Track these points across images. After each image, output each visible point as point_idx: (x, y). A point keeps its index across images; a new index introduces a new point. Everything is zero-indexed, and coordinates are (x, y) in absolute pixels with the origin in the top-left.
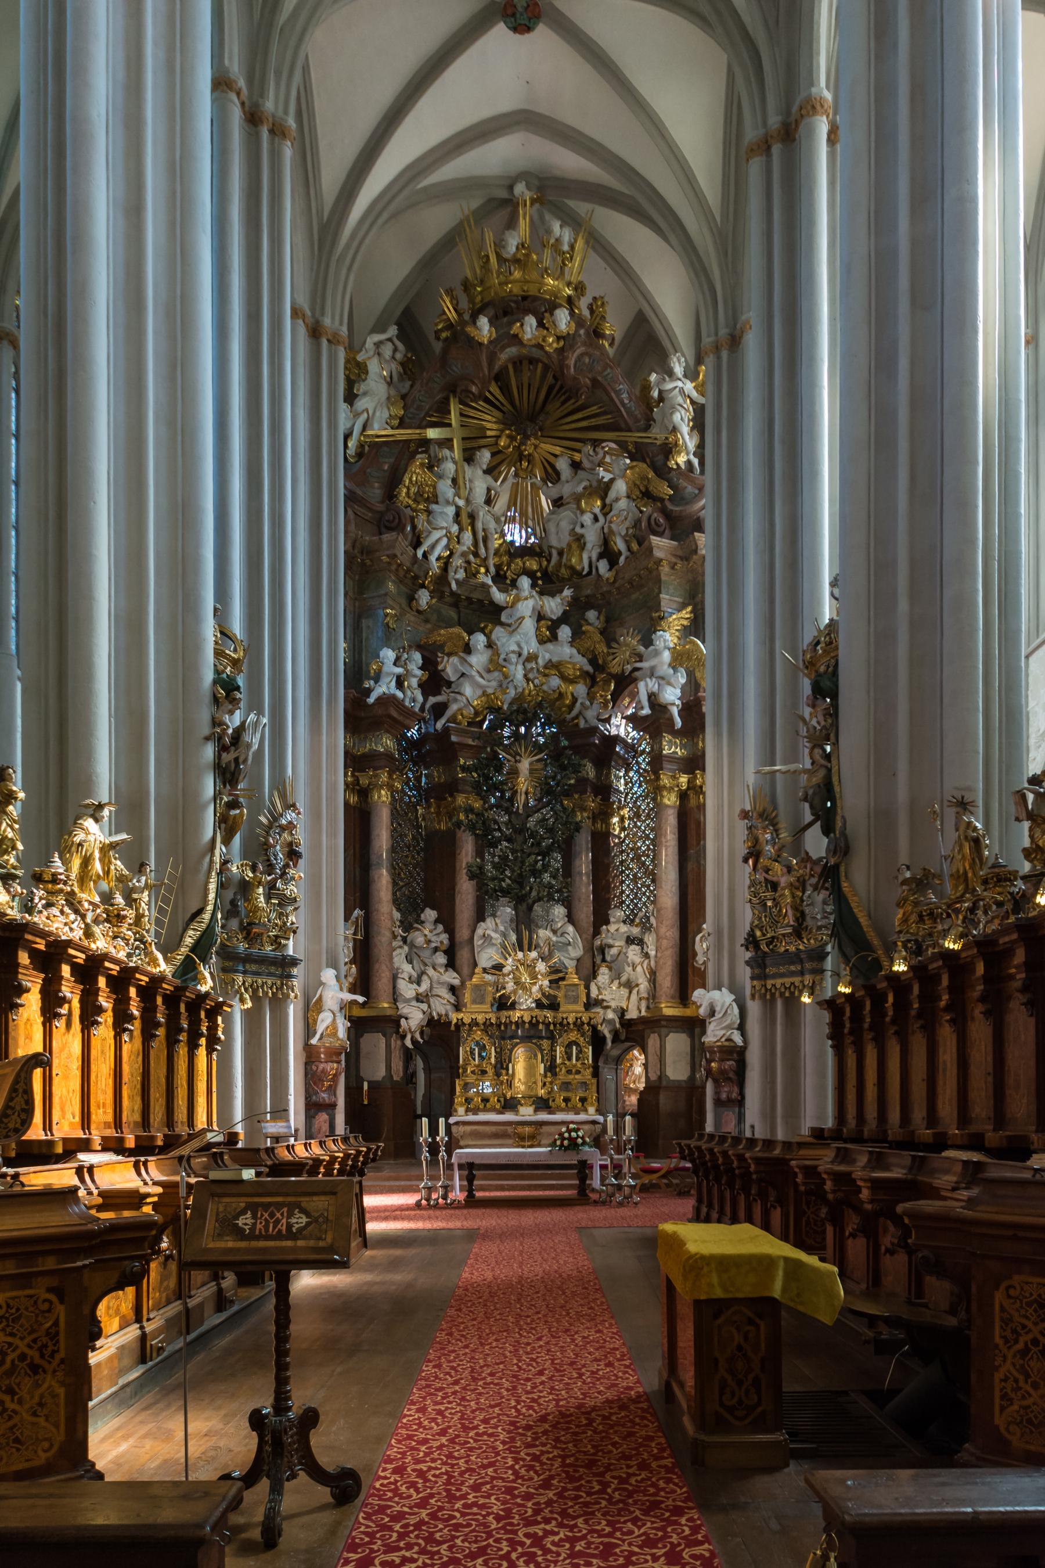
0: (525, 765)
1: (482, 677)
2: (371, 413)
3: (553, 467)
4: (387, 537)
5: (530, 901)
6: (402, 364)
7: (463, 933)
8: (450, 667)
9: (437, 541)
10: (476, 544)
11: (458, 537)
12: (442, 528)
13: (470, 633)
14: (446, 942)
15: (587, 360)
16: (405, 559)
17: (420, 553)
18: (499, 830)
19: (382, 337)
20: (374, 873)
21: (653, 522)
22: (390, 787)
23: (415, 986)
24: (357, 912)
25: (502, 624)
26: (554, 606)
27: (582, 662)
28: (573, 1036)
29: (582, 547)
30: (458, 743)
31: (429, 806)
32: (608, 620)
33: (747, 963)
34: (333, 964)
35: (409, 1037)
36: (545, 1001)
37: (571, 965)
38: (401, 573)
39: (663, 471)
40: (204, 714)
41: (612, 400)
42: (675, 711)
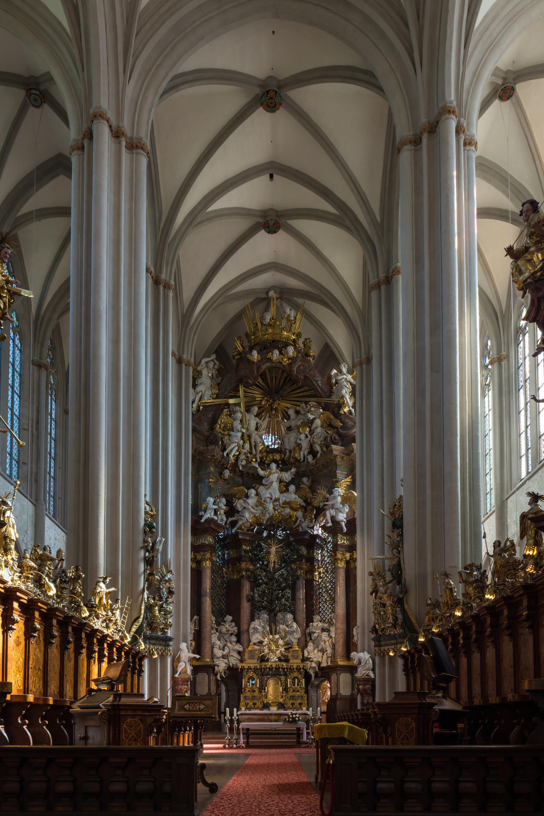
0: (273, 549)
1: (254, 509)
2: (203, 392)
3: (287, 413)
4: (210, 447)
5: (276, 612)
6: (217, 370)
7: (244, 627)
8: (239, 504)
9: (233, 448)
11: (243, 446)
12: (235, 442)
13: (248, 489)
14: (236, 631)
15: (302, 368)
16: (218, 457)
17: (225, 454)
18: (261, 579)
20: (203, 599)
21: (333, 438)
22: (211, 560)
23: (222, 651)
24: (195, 617)
25: (263, 485)
26: (287, 476)
27: (300, 501)
28: (296, 674)
29: (300, 449)
30: (242, 539)
31: (228, 568)
32: (312, 482)
33: (373, 639)
34: (185, 641)
35: (219, 675)
36: (283, 658)
37: (295, 641)
38: (217, 463)
39: (337, 415)
40: (140, 538)
41: (314, 385)
42: (343, 524)
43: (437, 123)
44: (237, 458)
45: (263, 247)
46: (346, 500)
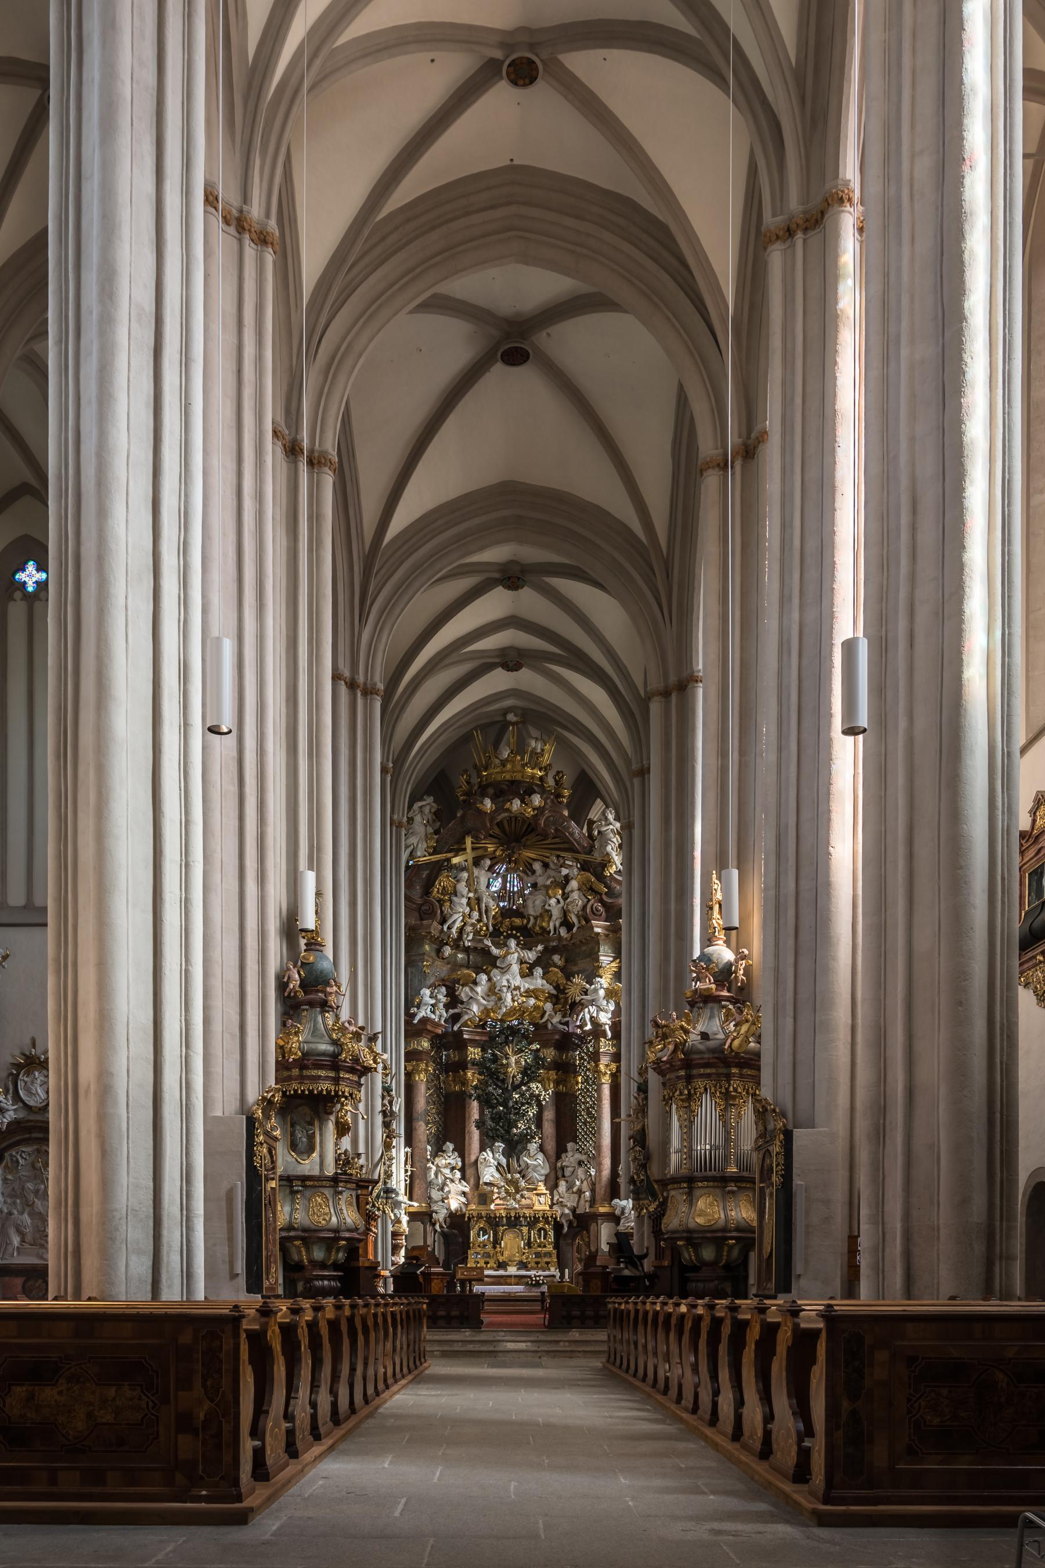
8: (464, 993)
10: (480, 915)
14: (460, 1164)
19: (424, 803)
22: (426, 1071)
25: (498, 967)
26: (531, 956)
27: (549, 988)
29: (551, 916)
31: (448, 1076)
32: (566, 961)
43: (823, 213)
44: (461, 930)
45: (498, 681)
46: (610, 994)
